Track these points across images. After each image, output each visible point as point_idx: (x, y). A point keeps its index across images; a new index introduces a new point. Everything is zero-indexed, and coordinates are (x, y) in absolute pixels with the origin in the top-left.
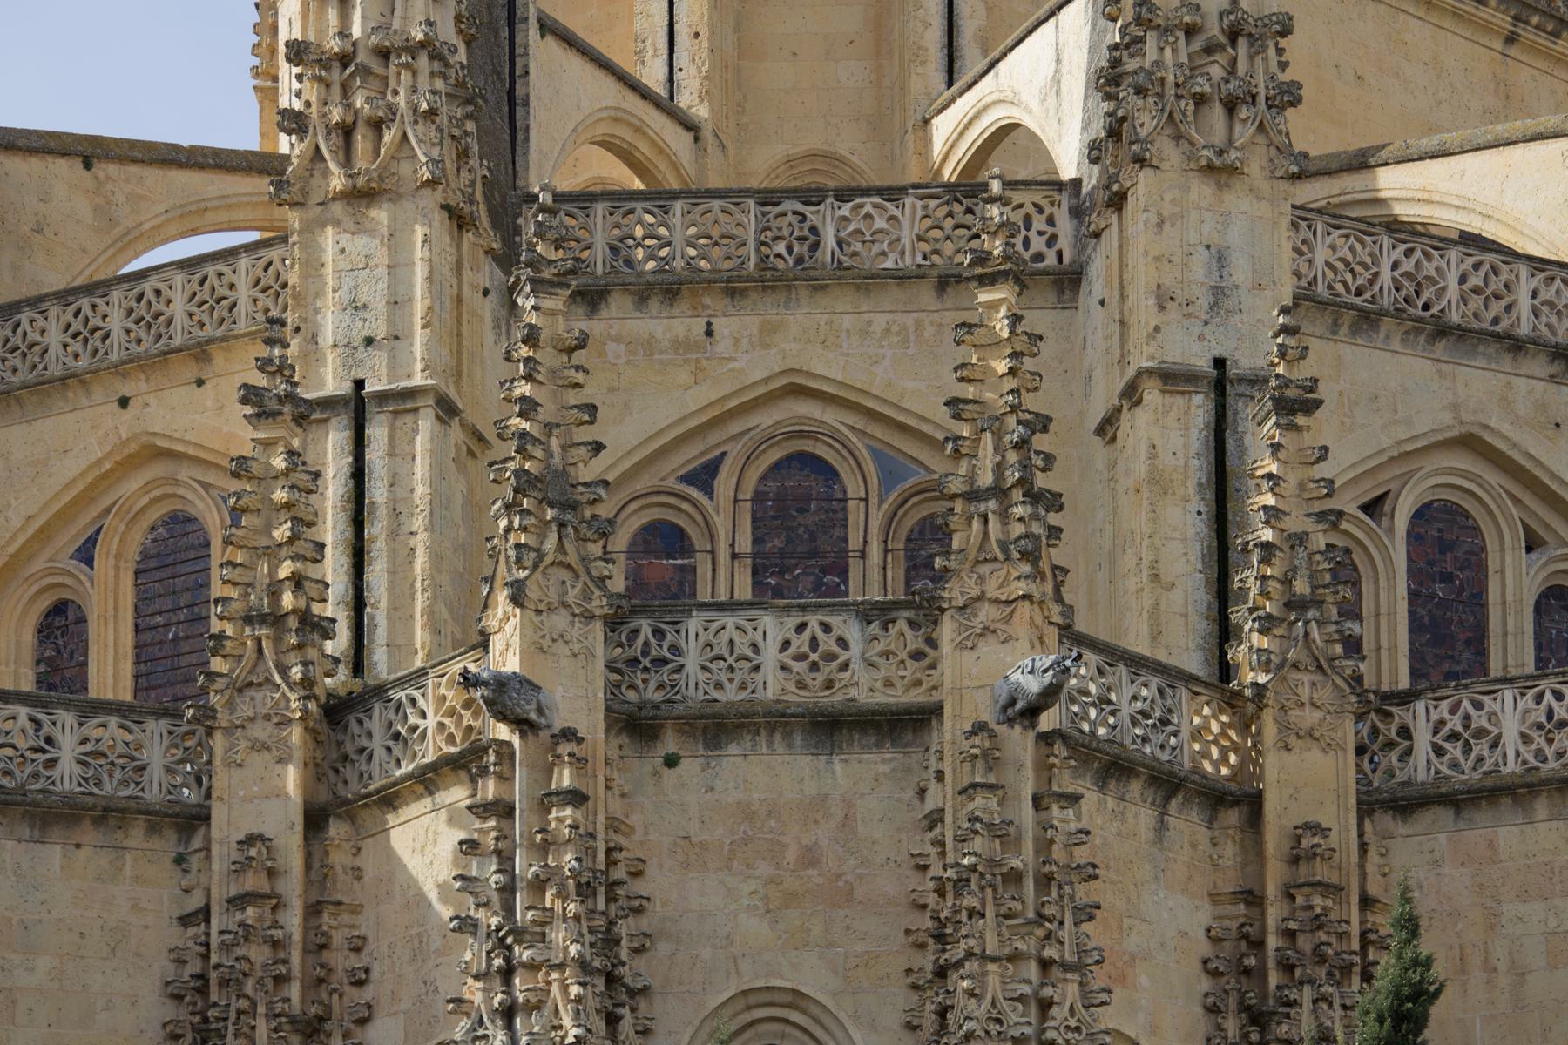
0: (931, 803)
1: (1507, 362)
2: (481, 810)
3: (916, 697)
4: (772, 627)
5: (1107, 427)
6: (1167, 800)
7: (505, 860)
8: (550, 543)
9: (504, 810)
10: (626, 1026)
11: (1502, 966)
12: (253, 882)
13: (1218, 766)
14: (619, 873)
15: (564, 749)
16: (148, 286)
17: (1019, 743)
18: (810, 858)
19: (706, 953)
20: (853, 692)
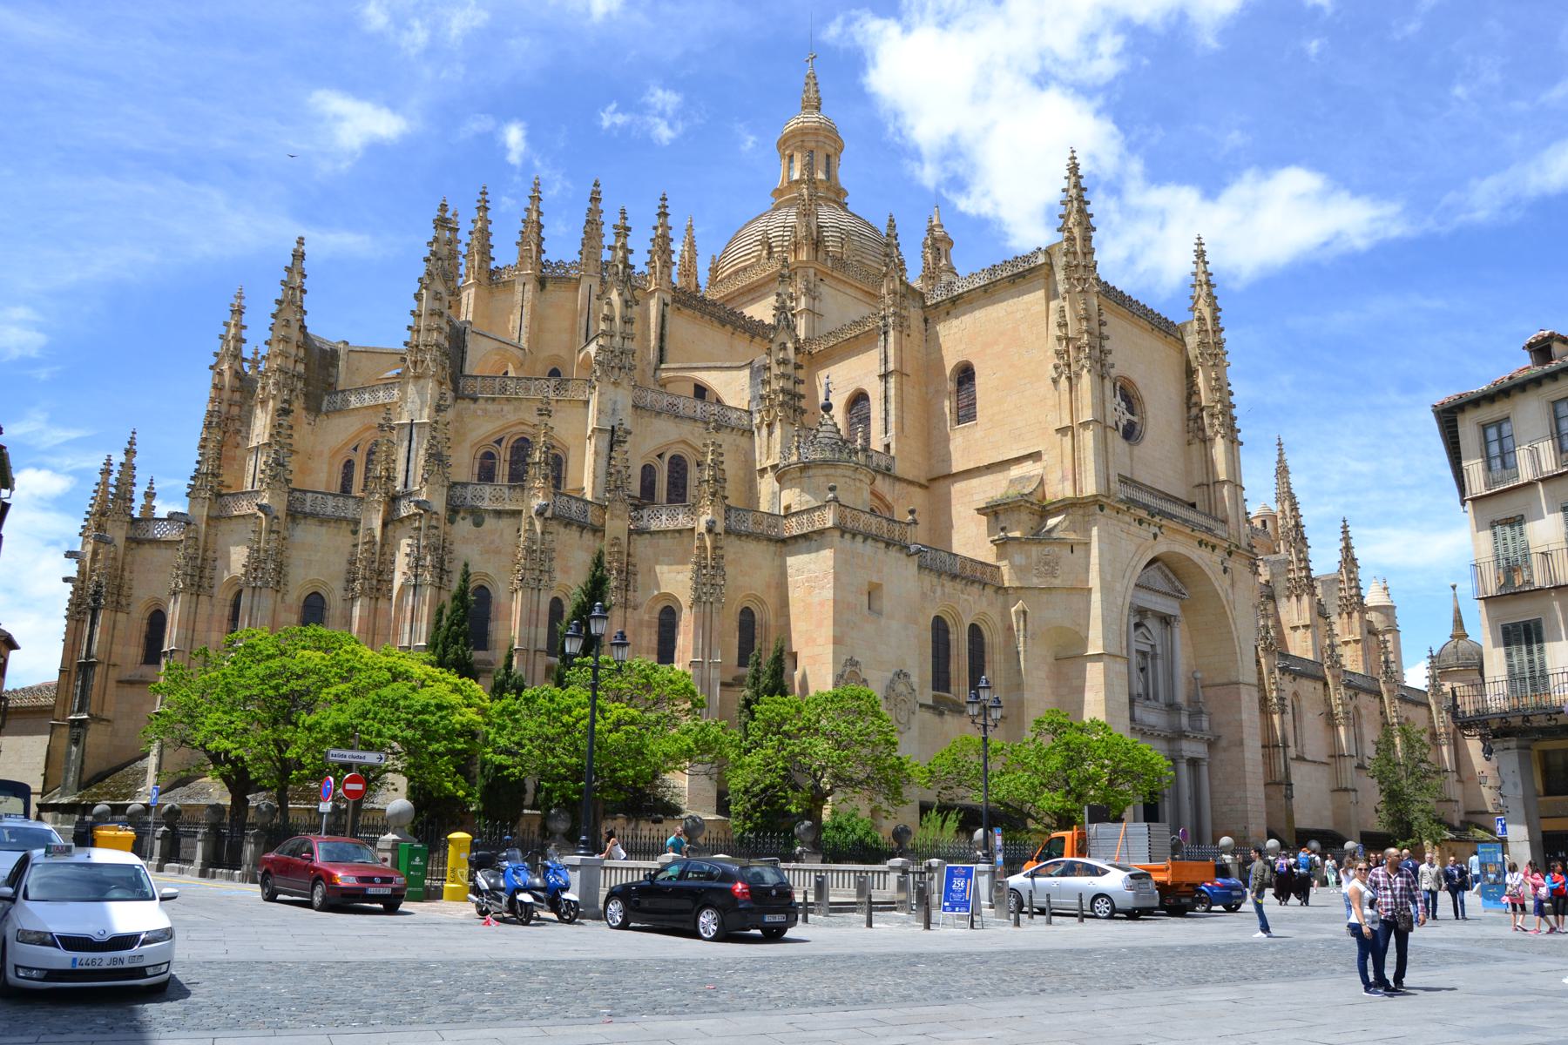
1: (693, 424)
3: (520, 508)
4: (487, 490)
6: (582, 532)
8: (436, 468)
13: (597, 523)
14: (447, 545)
15: (434, 516)
18: (492, 542)
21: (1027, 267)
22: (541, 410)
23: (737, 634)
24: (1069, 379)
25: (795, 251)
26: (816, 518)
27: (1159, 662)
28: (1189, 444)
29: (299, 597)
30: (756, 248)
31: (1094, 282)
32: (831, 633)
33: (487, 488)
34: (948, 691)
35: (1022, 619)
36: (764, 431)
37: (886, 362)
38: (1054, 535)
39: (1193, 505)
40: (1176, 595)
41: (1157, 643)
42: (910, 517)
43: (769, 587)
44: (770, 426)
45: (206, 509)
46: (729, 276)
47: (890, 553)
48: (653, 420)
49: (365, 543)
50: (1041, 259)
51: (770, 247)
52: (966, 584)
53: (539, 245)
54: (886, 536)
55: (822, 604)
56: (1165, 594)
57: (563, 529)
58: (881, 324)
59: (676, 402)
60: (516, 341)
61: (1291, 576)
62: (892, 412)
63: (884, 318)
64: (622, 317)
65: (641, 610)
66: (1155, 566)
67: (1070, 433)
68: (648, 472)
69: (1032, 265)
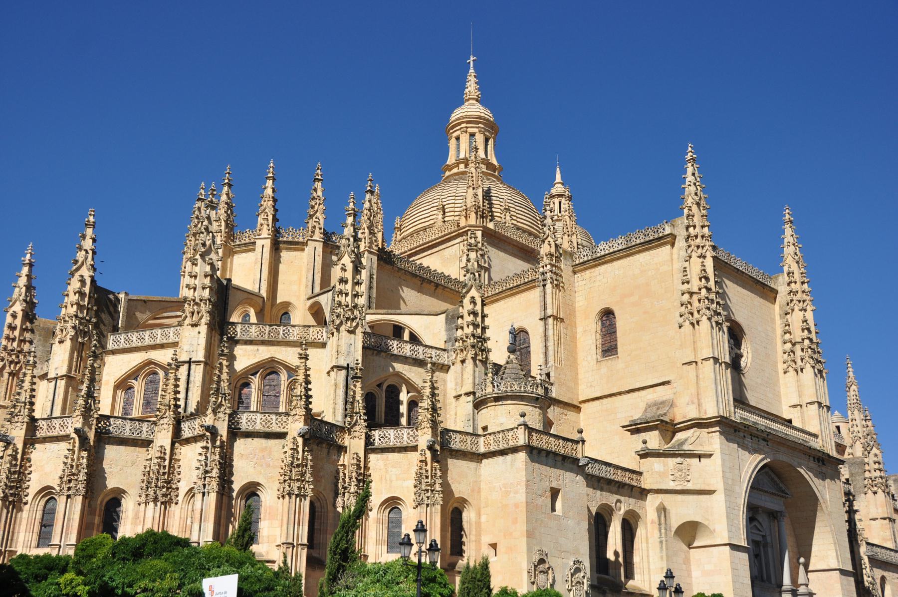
0: (285, 450)
1: (405, 360)
2: (203, 448)
3: (285, 430)
4: (259, 416)
5: (328, 373)
6: (329, 449)
7: (207, 457)
9: (206, 448)
10: (226, 489)
11: (388, 479)
12: (162, 455)
16: (153, 331)
17: (300, 441)
19: (242, 475)
20: (273, 428)
21: (656, 236)
22: (301, 355)
23: (450, 528)
24: (692, 324)
25: (466, 217)
26: (510, 437)
27: (770, 550)
28: (785, 373)
29: (101, 503)
30: (433, 213)
31: (710, 248)
32: (525, 528)
33: (259, 415)
34: (607, 573)
35: (663, 515)
36: (458, 365)
37: (545, 309)
38: (685, 447)
39: (790, 421)
40: (782, 493)
41: (767, 534)
42: (579, 435)
43: (473, 491)
44: (463, 362)
45: (23, 431)
46: (411, 235)
47: (565, 464)
48: (376, 358)
49: (157, 458)
50: (668, 230)
51: (444, 213)
52: (619, 487)
53: (274, 216)
54: (562, 452)
55: (516, 506)
56: (773, 494)
57: (316, 447)
58: (541, 278)
59: (391, 343)
60: (257, 291)
61: (867, 474)
62: (551, 348)
63: (543, 274)
64: (353, 279)
65: (375, 510)
66: (764, 471)
67: (694, 364)
68: (369, 399)
69: (661, 235)
